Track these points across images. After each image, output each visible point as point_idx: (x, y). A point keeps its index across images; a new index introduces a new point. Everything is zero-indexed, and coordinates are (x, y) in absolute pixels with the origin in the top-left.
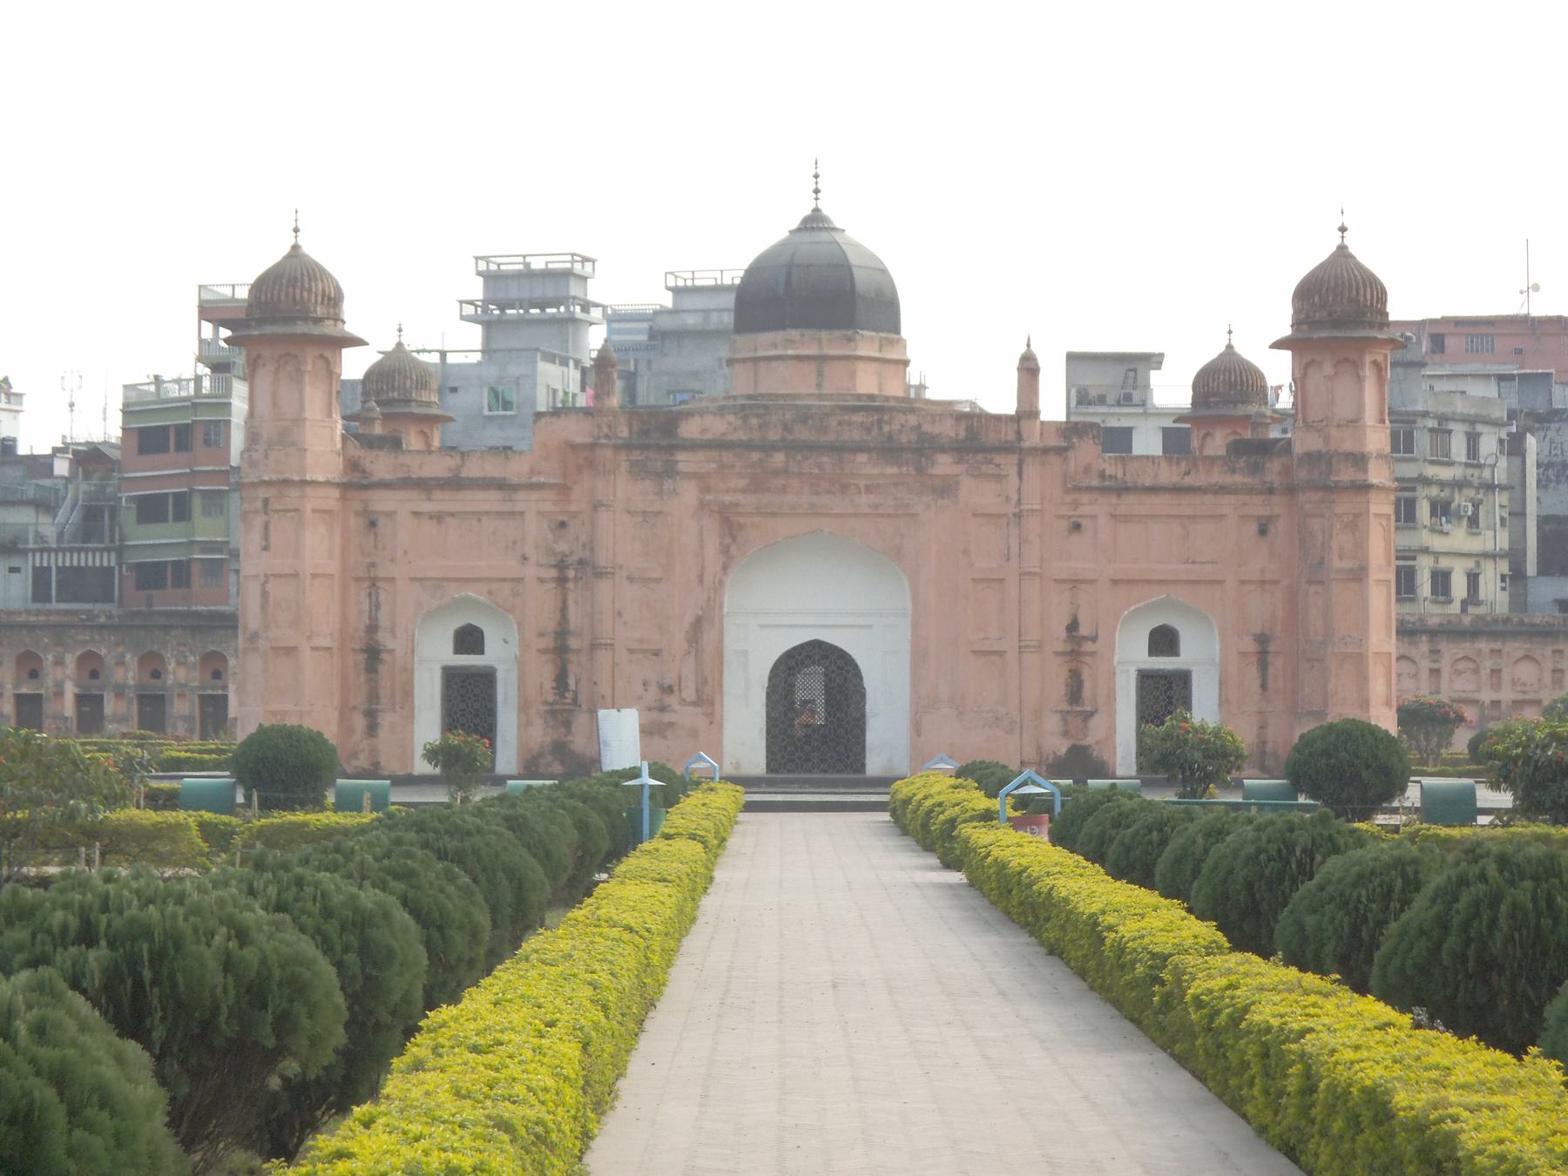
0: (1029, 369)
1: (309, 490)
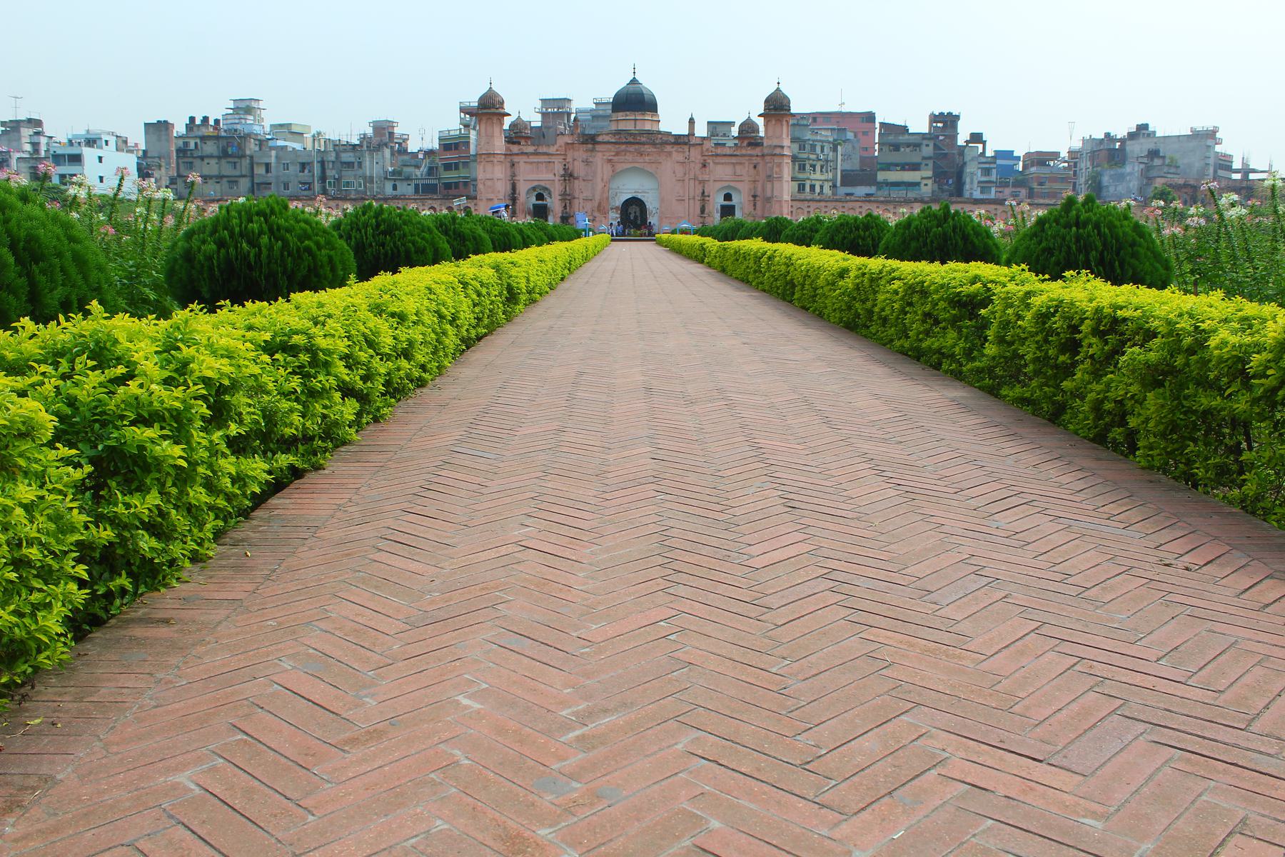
0: (692, 121)
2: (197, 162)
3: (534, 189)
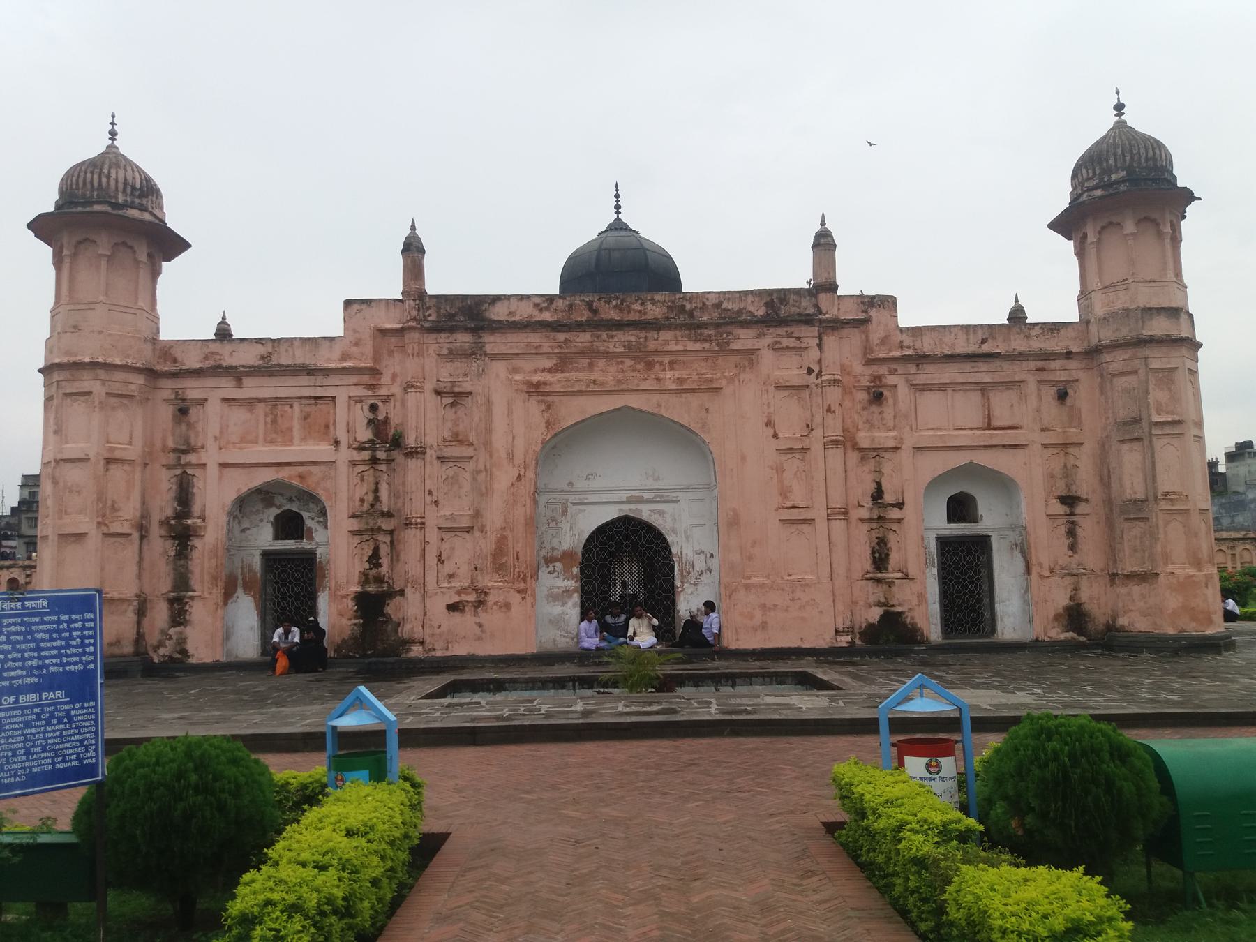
1: (102, 373)
3: (265, 494)
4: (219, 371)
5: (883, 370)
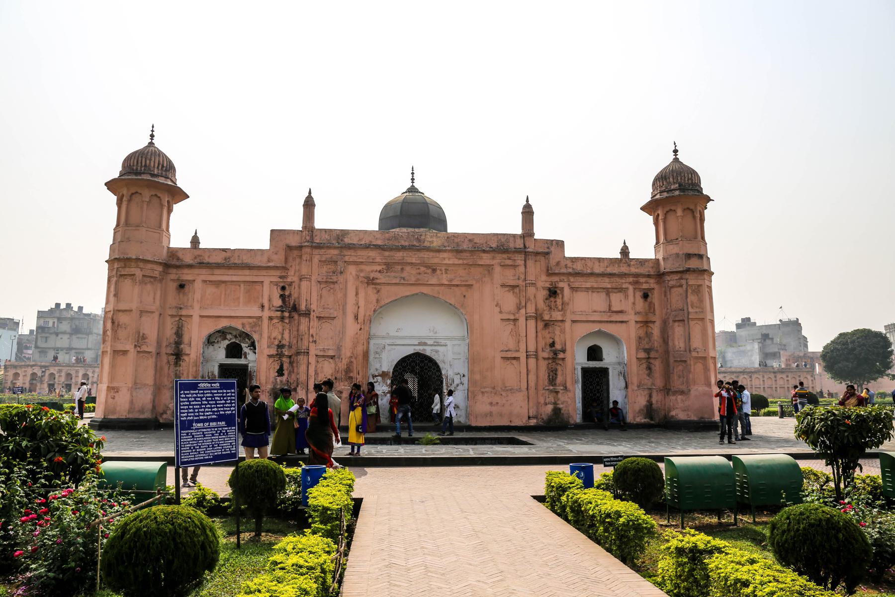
0: (528, 213)
1: (141, 265)
2: (54, 336)
3: (222, 333)
4: (202, 265)
5: (555, 279)
